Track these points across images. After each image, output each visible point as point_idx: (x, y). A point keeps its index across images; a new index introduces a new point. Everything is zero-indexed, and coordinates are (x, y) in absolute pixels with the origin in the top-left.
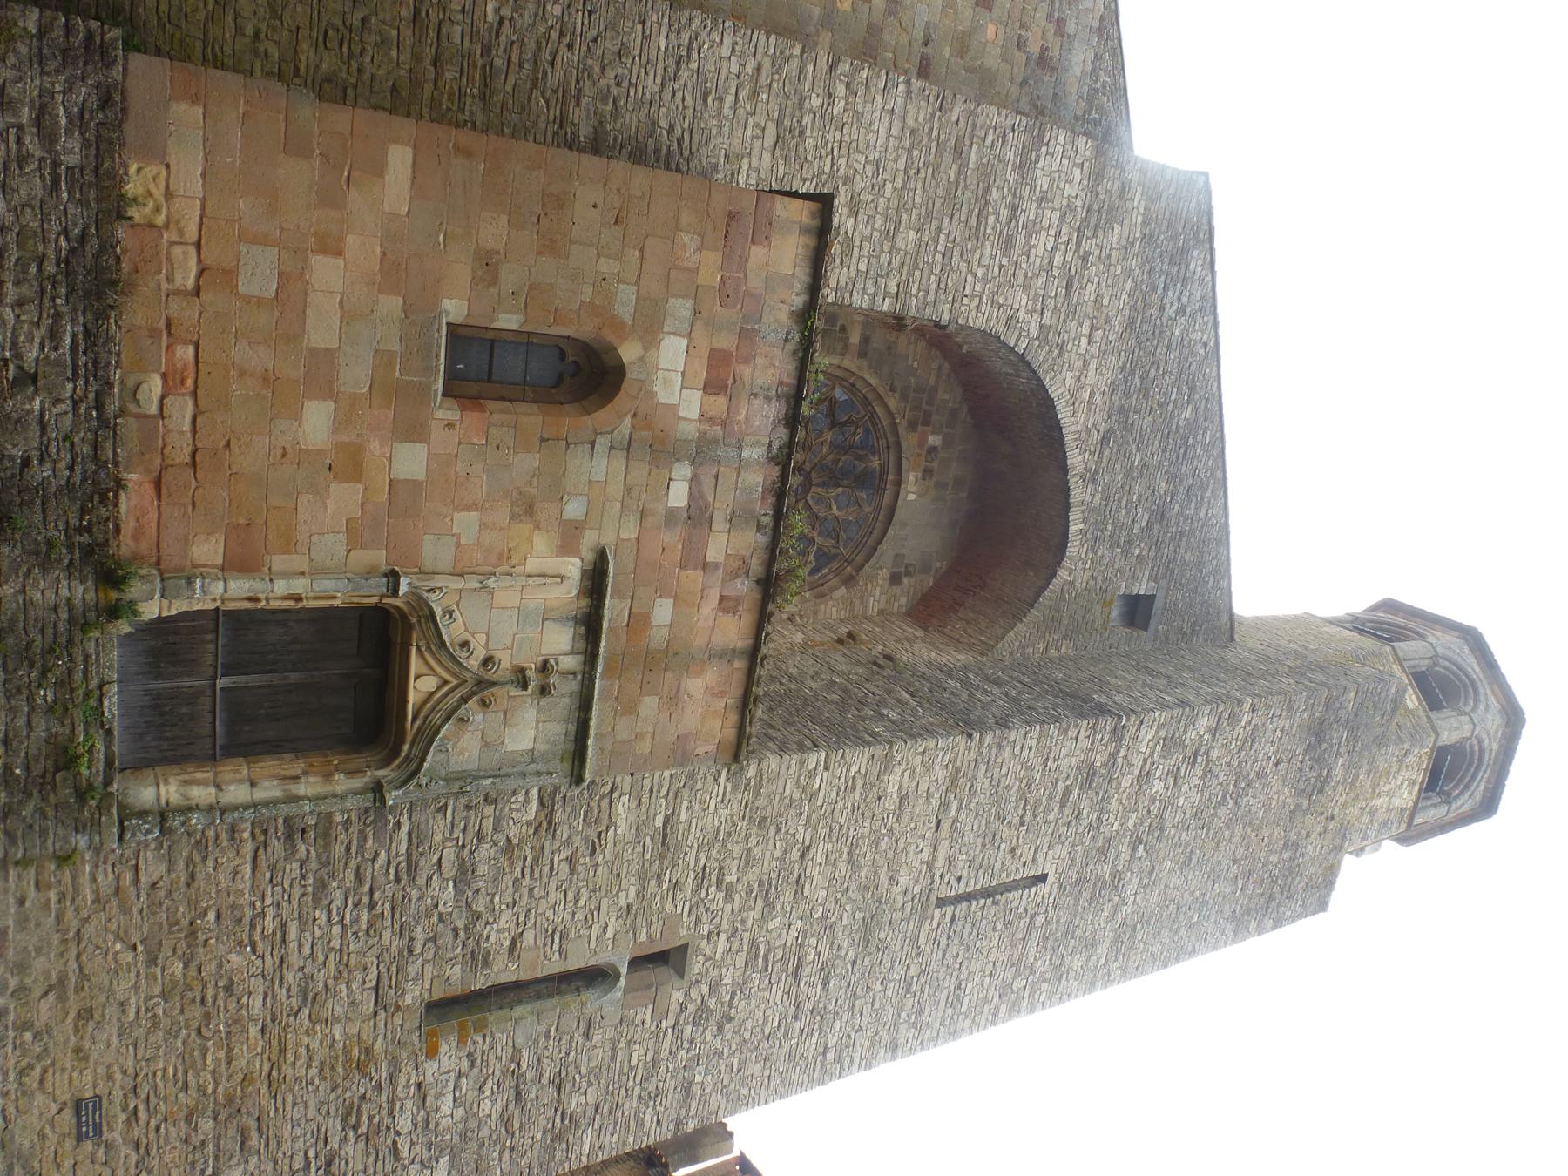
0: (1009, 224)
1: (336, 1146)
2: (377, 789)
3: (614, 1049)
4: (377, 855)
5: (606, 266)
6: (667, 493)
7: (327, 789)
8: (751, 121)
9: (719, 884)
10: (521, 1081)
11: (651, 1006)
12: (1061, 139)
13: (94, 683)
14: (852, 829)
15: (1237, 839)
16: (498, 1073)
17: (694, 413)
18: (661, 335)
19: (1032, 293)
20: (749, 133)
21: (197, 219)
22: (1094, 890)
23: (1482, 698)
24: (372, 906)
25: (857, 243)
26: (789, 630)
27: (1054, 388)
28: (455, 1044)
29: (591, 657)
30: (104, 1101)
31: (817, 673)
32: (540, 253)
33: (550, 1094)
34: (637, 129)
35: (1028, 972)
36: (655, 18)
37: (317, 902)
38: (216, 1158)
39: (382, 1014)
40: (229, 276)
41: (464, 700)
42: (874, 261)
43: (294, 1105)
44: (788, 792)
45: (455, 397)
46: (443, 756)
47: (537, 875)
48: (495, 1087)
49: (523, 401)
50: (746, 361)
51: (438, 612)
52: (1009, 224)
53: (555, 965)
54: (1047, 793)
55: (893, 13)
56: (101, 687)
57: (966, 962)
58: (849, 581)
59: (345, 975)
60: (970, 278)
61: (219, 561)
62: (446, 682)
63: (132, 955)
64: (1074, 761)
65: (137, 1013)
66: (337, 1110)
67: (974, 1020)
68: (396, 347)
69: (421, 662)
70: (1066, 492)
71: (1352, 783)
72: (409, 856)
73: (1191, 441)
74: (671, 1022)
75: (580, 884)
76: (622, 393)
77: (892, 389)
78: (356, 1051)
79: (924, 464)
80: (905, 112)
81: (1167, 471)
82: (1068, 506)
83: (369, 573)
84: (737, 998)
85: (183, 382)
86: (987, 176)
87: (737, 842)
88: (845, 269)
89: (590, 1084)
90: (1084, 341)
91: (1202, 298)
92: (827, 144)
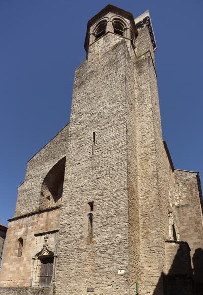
33: (109, 219)
40: (11, 278)
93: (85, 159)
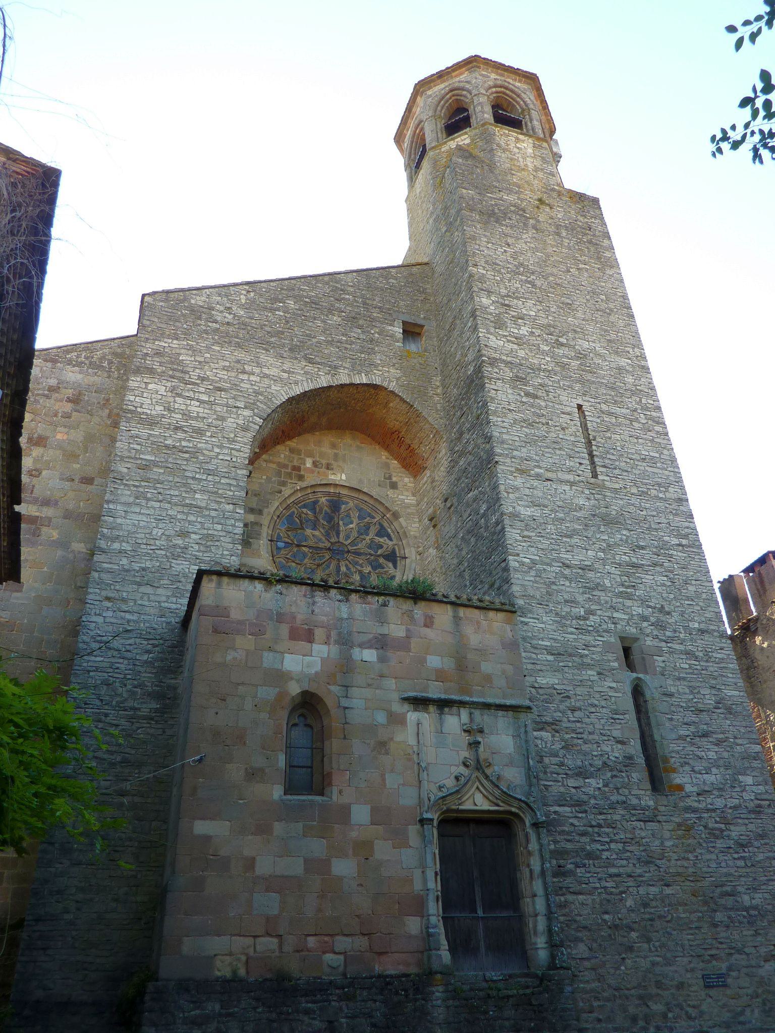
0: (186, 432)
1: (732, 841)
2: (536, 825)
3: (679, 679)
4: (572, 824)
5: (248, 705)
6: (370, 662)
7: (537, 853)
8: (140, 602)
9: (585, 619)
10: (696, 734)
11: (655, 657)
12: (132, 398)
13: (484, 985)
14: (553, 536)
15: (555, 271)
16: (692, 749)
17: (325, 648)
18: (284, 669)
19: (226, 415)
20: (146, 603)
21: (241, 938)
22: (586, 371)
23: (461, 85)
24: (600, 826)
25: (205, 532)
26: (427, 557)
27: (282, 398)
28: (676, 775)
29: (462, 704)
30: (705, 973)
31: (457, 546)
32: (245, 743)
33: (705, 716)
34: (150, 673)
35: (635, 413)
36: (85, 664)
37: (598, 858)
38: (738, 910)
39: (660, 818)
41: (487, 777)
42: (216, 520)
43: (709, 867)
44: (532, 579)
45: (323, 789)
46: (518, 790)
47: (581, 730)
48: (700, 750)
49: (323, 749)
50: (294, 618)
51: (441, 794)
52: (186, 432)
53: (631, 716)
54: (529, 408)
55: (56, 503)
56: (487, 981)
57: (630, 456)
58: (396, 516)
59: (638, 840)
60: (220, 457)
61: (418, 919)
62: (478, 788)
63: (627, 960)
64: (510, 391)
65: (658, 956)
66: (712, 842)
67: (664, 448)
68: (301, 825)
69: (467, 803)
70: (342, 386)
71: (519, 187)
72: (572, 806)
73: (307, 300)
74: (664, 644)
75: (586, 704)
76: (316, 692)
77: (280, 492)
78: (680, 832)
79: (323, 470)
80: (124, 504)
81: (326, 315)
82: (352, 385)
83: (423, 837)
84: (650, 604)
85: (326, 942)
86: (159, 447)
87: (561, 609)
88: (222, 538)
89: (699, 692)
90: (252, 378)
91: (220, 295)
92: (148, 553)
93: (570, 477)
